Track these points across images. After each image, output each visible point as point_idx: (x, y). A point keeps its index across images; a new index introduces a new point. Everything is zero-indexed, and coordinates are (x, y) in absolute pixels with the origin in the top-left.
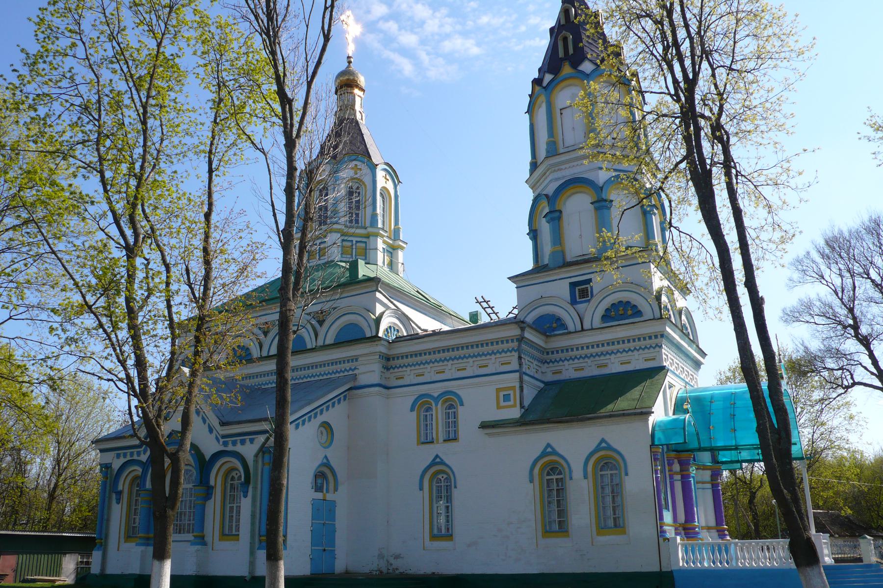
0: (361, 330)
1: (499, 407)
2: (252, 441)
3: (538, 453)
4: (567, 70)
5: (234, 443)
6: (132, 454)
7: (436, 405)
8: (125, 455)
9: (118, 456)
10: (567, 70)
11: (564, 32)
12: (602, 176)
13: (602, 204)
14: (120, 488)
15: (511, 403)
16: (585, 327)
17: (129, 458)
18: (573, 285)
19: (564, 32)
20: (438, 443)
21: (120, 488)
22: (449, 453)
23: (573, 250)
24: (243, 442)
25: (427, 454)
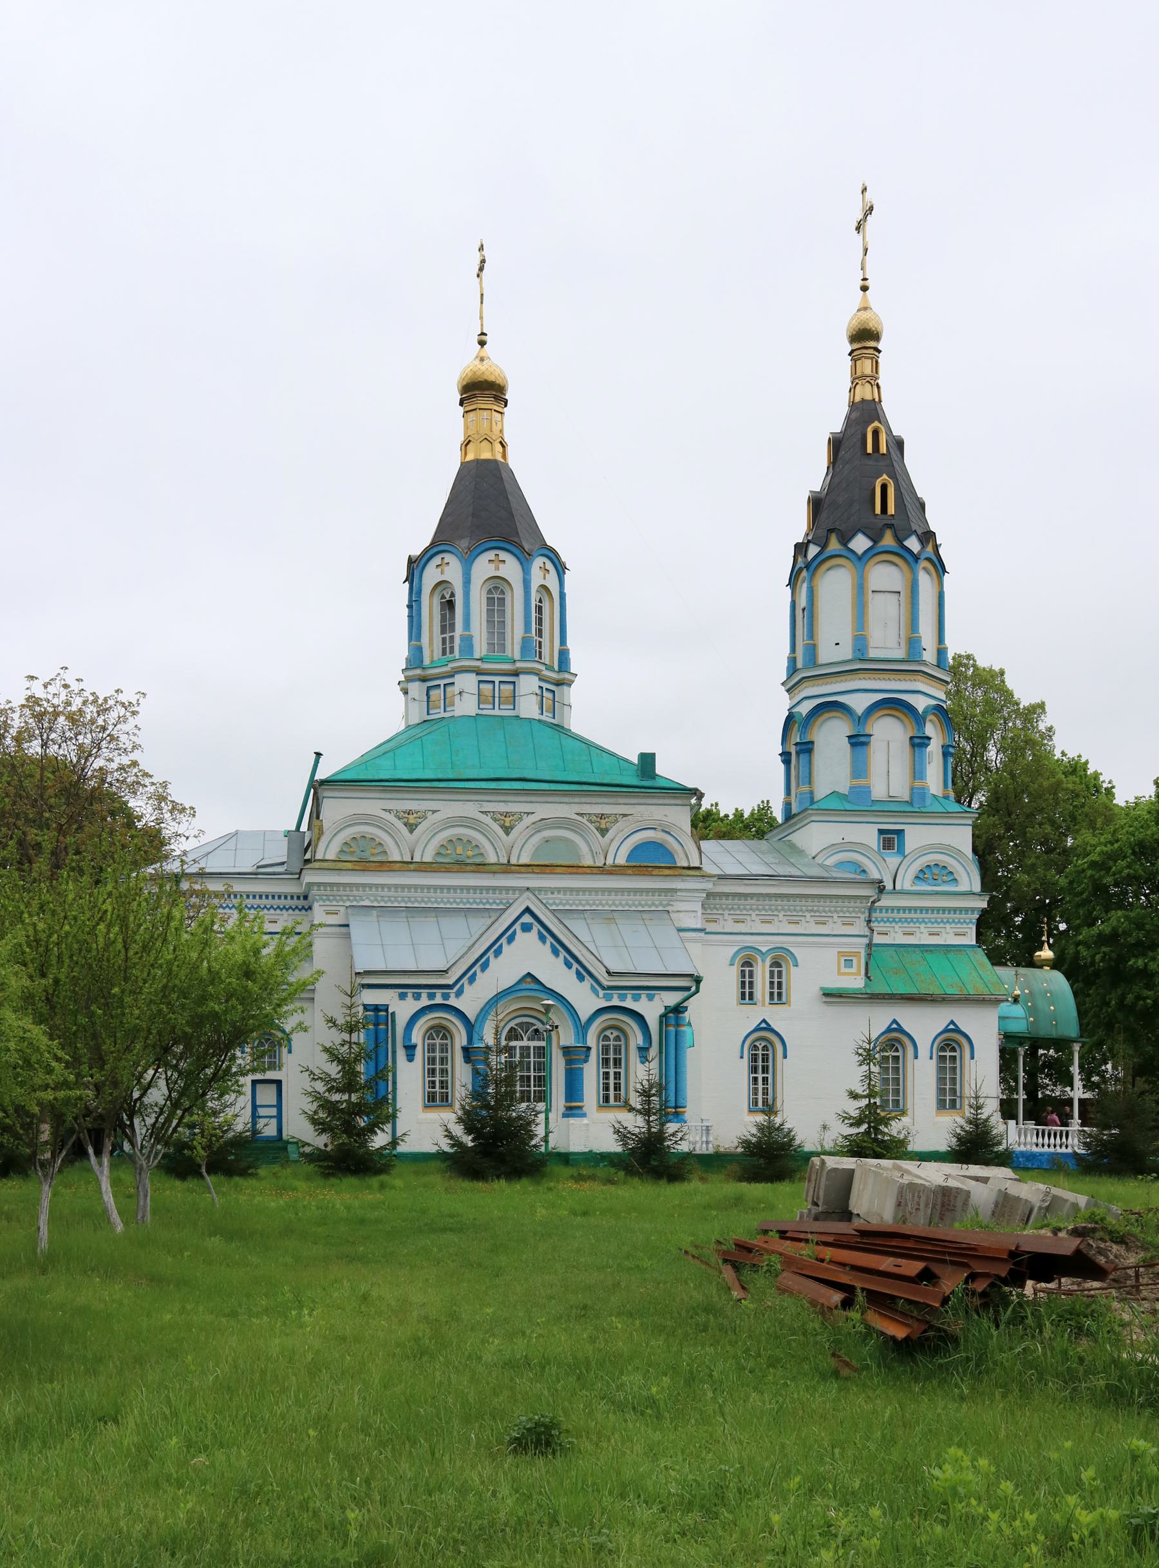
0: (670, 854)
1: (840, 973)
2: (651, 998)
3: (883, 1030)
4: (888, 540)
5: (623, 998)
6: (431, 996)
7: (763, 961)
8: (417, 997)
9: (402, 997)
10: (888, 540)
11: (885, 476)
14: (414, 1041)
15: (853, 970)
17: (425, 1001)
18: (881, 832)
19: (885, 476)
20: (764, 1005)
21: (414, 1041)
22: (778, 1018)
23: (879, 791)
24: (636, 998)
25: (752, 1017)
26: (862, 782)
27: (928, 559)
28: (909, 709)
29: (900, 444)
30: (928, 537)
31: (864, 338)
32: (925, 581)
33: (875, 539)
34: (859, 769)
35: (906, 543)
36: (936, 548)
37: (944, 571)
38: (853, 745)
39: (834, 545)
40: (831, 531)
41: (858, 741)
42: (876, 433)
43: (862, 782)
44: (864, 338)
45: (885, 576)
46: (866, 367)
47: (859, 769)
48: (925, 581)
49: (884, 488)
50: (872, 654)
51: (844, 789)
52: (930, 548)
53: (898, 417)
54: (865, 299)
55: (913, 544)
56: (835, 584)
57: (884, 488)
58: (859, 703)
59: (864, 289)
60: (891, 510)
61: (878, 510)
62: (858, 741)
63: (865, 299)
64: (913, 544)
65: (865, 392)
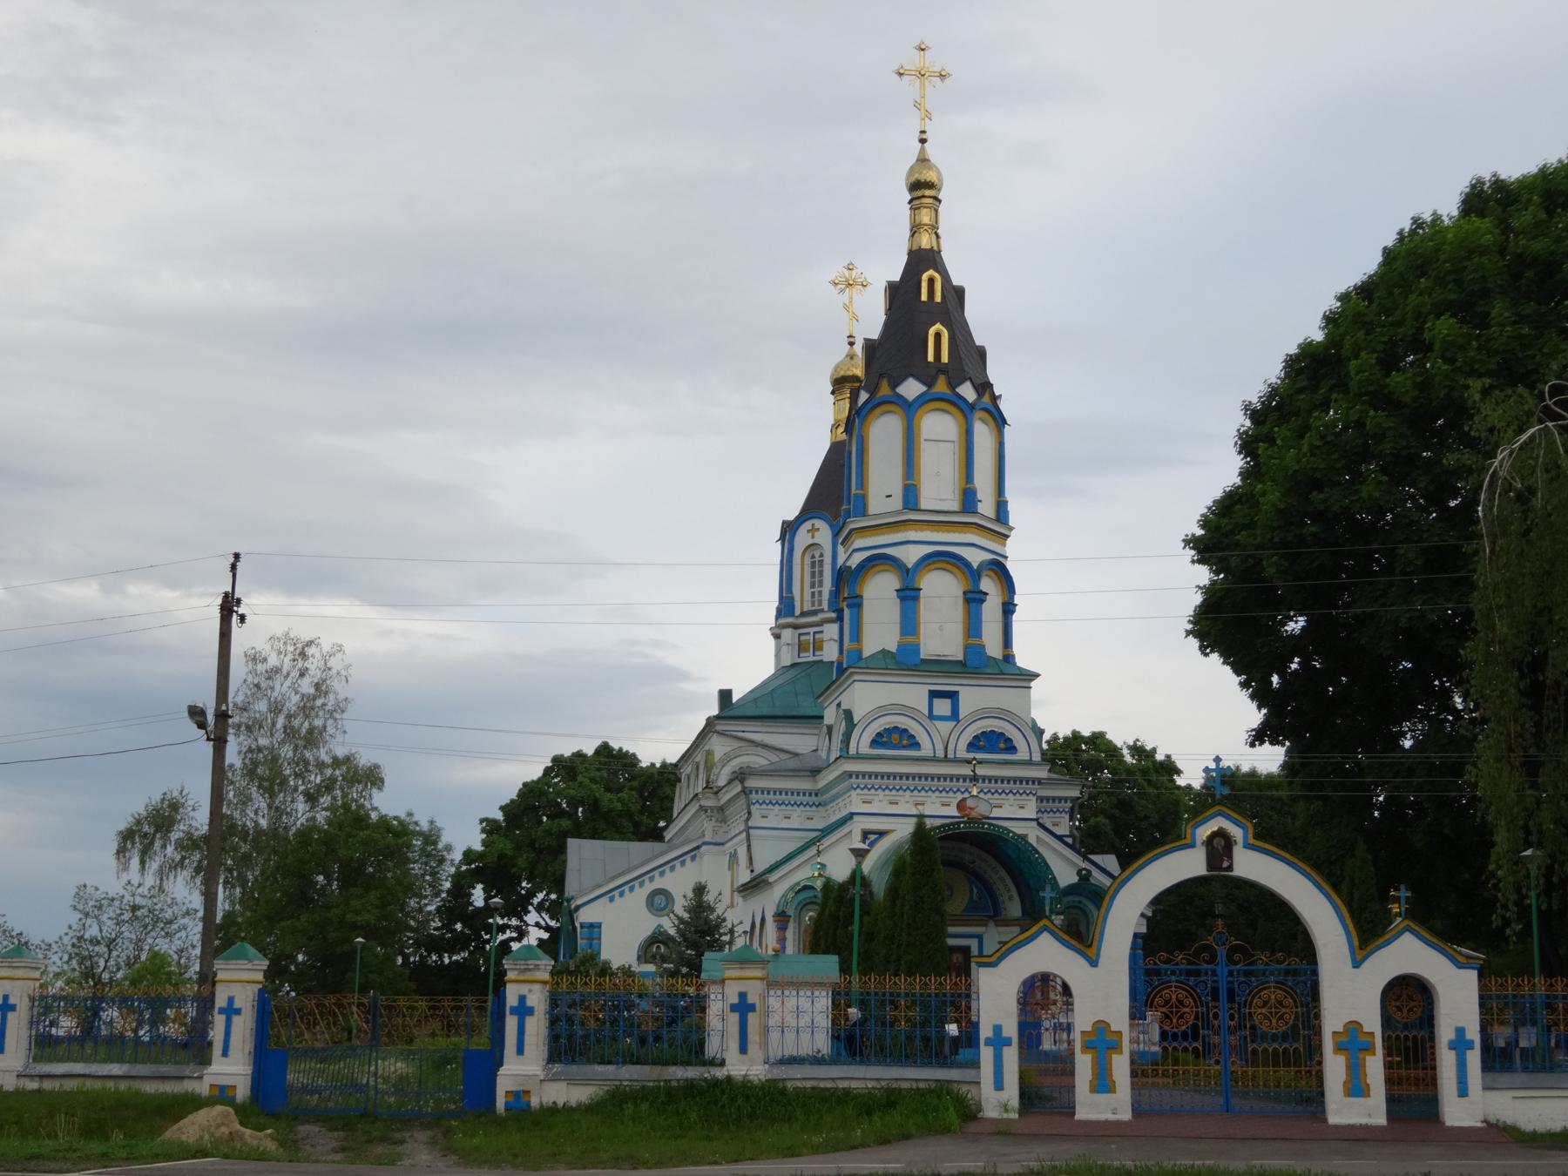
4: (941, 386)
10: (941, 386)
12: (975, 558)
13: (974, 599)
16: (951, 756)
26: (911, 639)
27: (986, 410)
28: (967, 564)
29: (960, 293)
30: (984, 387)
31: (922, 189)
32: (982, 433)
33: (929, 382)
34: (909, 623)
36: (995, 399)
37: (1005, 422)
39: (885, 390)
40: (882, 375)
41: (909, 595)
43: (911, 639)
44: (922, 189)
45: (938, 426)
46: (925, 217)
47: (909, 623)
48: (982, 433)
49: (938, 336)
50: (923, 506)
51: (892, 647)
52: (986, 399)
54: (923, 151)
55: (967, 391)
57: (938, 336)
58: (911, 555)
59: (923, 141)
60: (945, 358)
61: (931, 358)
62: (909, 595)
63: (923, 151)
64: (967, 391)
65: (925, 241)
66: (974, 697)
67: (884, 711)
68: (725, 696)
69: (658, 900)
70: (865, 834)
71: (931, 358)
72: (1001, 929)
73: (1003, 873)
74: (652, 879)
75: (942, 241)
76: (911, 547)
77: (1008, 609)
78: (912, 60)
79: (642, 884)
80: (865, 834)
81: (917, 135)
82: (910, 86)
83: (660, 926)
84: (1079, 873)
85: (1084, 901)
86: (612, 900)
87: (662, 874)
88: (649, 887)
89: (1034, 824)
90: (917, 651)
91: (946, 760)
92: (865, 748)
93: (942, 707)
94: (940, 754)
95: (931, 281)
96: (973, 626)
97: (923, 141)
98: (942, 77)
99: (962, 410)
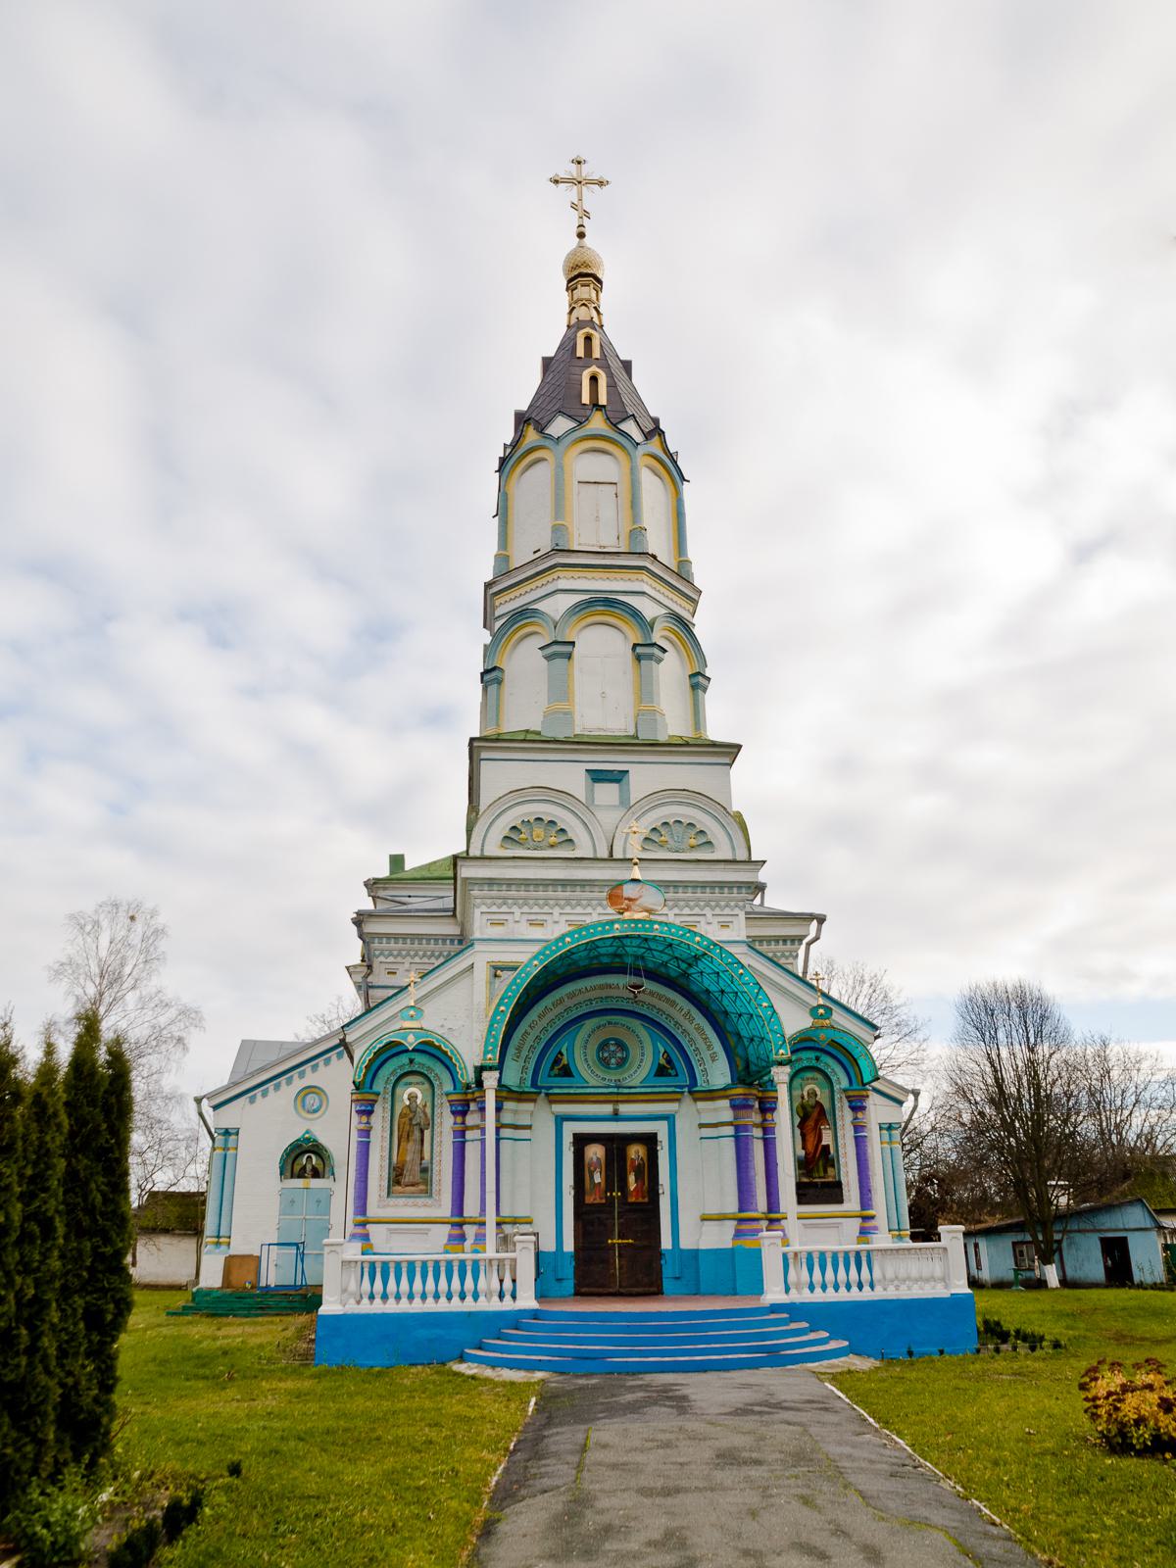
4: (597, 423)
10: (597, 423)
12: (649, 610)
16: (617, 855)
28: (635, 614)
31: (582, 276)
34: (561, 690)
35: (622, 426)
38: (548, 658)
42: (588, 339)
44: (582, 276)
49: (594, 379)
53: (621, 334)
56: (535, 481)
57: (594, 379)
60: (603, 400)
61: (586, 399)
64: (629, 426)
65: (582, 313)
66: (646, 776)
67: (520, 795)
68: (397, 861)
69: (312, 1100)
70: (497, 970)
71: (586, 399)
72: (701, 1105)
73: (700, 1020)
74: (302, 1075)
75: (603, 318)
76: (559, 596)
77: (698, 682)
78: (568, 170)
79: (289, 1082)
80: (497, 970)
81: (575, 231)
82: (570, 193)
83: (307, 1132)
84: (813, 1011)
85: (825, 1058)
86: (252, 1100)
87: (315, 1068)
88: (298, 1084)
89: (744, 949)
90: (572, 722)
91: (611, 858)
92: (493, 849)
93: (607, 792)
94: (603, 853)
95: (588, 339)
96: (644, 691)
97: (581, 235)
98: (601, 183)
99: (623, 447)
